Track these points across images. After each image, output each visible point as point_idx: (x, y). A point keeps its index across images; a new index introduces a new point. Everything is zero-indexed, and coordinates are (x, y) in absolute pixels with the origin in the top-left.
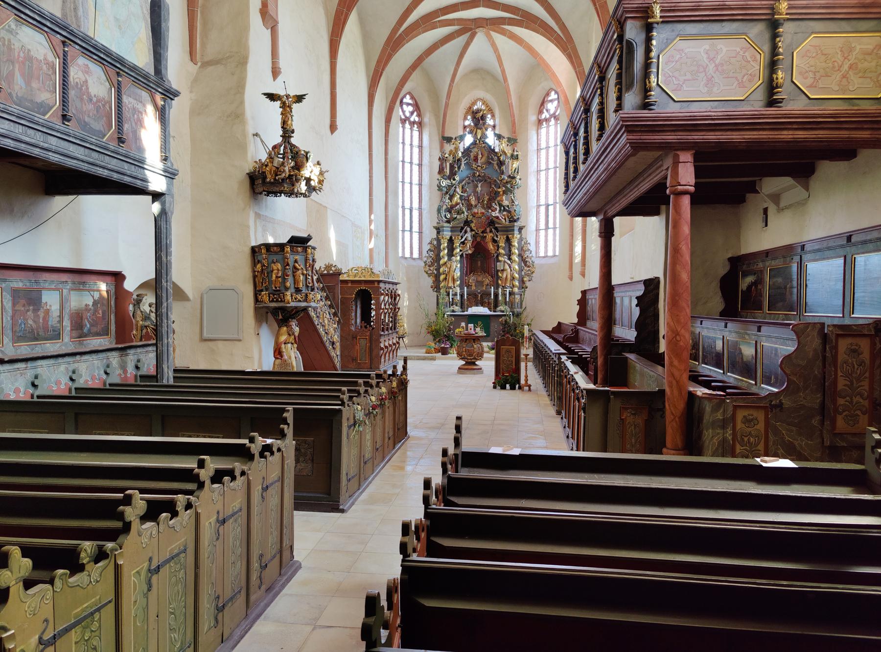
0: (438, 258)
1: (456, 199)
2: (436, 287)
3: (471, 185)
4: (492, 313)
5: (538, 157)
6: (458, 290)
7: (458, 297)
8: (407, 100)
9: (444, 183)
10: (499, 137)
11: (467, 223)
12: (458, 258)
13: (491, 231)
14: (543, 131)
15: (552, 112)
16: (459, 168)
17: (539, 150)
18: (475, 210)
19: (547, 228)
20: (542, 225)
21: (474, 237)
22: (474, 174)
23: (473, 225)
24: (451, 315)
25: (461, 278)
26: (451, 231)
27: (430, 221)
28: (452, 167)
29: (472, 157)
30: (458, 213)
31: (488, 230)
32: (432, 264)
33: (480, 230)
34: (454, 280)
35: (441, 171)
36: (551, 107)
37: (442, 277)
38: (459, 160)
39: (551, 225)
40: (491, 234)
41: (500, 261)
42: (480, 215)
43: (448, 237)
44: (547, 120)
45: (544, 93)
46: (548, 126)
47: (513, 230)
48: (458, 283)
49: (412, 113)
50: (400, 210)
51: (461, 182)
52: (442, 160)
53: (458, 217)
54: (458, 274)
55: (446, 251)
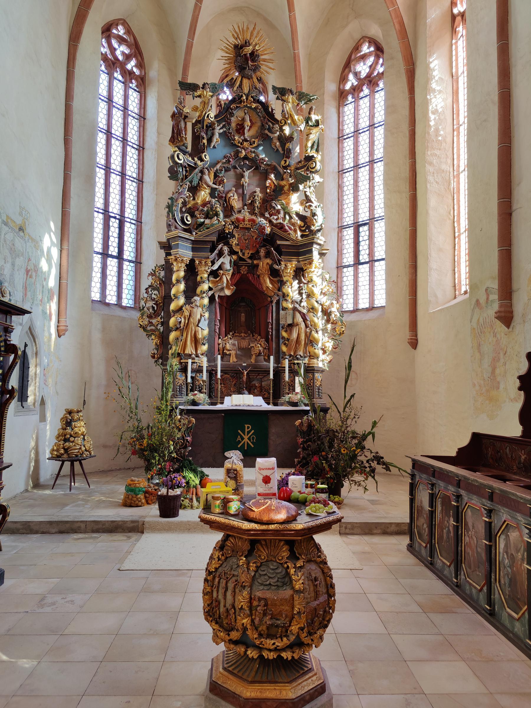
0: (167, 299)
1: (204, 195)
2: (161, 355)
3: (232, 173)
4: (271, 407)
5: (340, 150)
6: (204, 362)
7: (205, 375)
8: (121, 31)
9: (182, 159)
10: (282, 93)
11: (223, 237)
12: (206, 301)
13: (268, 255)
14: (349, 110)
15: (363, 75)
16: (210, 140)
17: (341, 138)
18: (241, 216)
19: (357, 263)
20: (349, 258)
21: (236, 265)
22: (237, 153)
23: (234, 242)
24: (189, 412)
25: (210, 339)
26: (194, 250)
27: (155, 232)
28: (196, 138)
29: (233, 125)
30: (207, 216)
31: (262, 252)
32: (156, 314)
33: (248, 253)
34: (196, 342)
35: (176, 138)
36: (363, 69)
37: (173, 336)
38: (210, 127)
39: (364, 257)
40: (269, 261)
41: (284, 309)
42: (247, 224)
43: (187, 260)
44: (356, 90)
45: (351, 45)
46: (357, 99)
47: (311, 251)
48: (205, 348)
49: (128, 57)
50: (99, 218)
51: (213, 165)
52: (178, 117)
53: (207, 221)
54: (204, 331)
55: (182, 286)
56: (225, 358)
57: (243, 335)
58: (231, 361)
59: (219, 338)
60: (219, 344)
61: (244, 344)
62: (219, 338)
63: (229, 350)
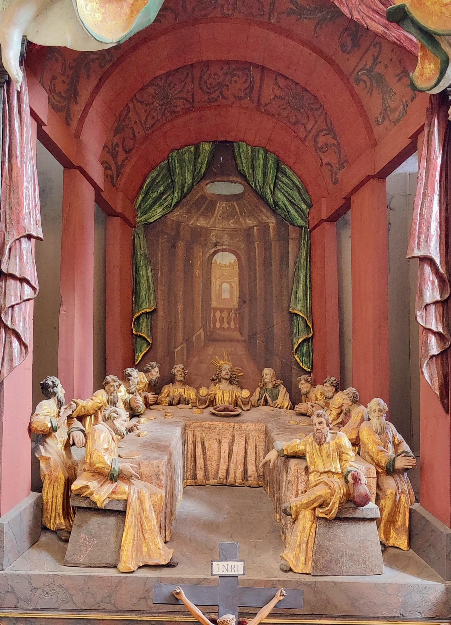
56: (79, 537)
57: (224, 393)
58: (129, 560)
59: (43, 391)
60: (39, 437)
61: (234, 445)
62: (43, 391)
63: (113, 477)
